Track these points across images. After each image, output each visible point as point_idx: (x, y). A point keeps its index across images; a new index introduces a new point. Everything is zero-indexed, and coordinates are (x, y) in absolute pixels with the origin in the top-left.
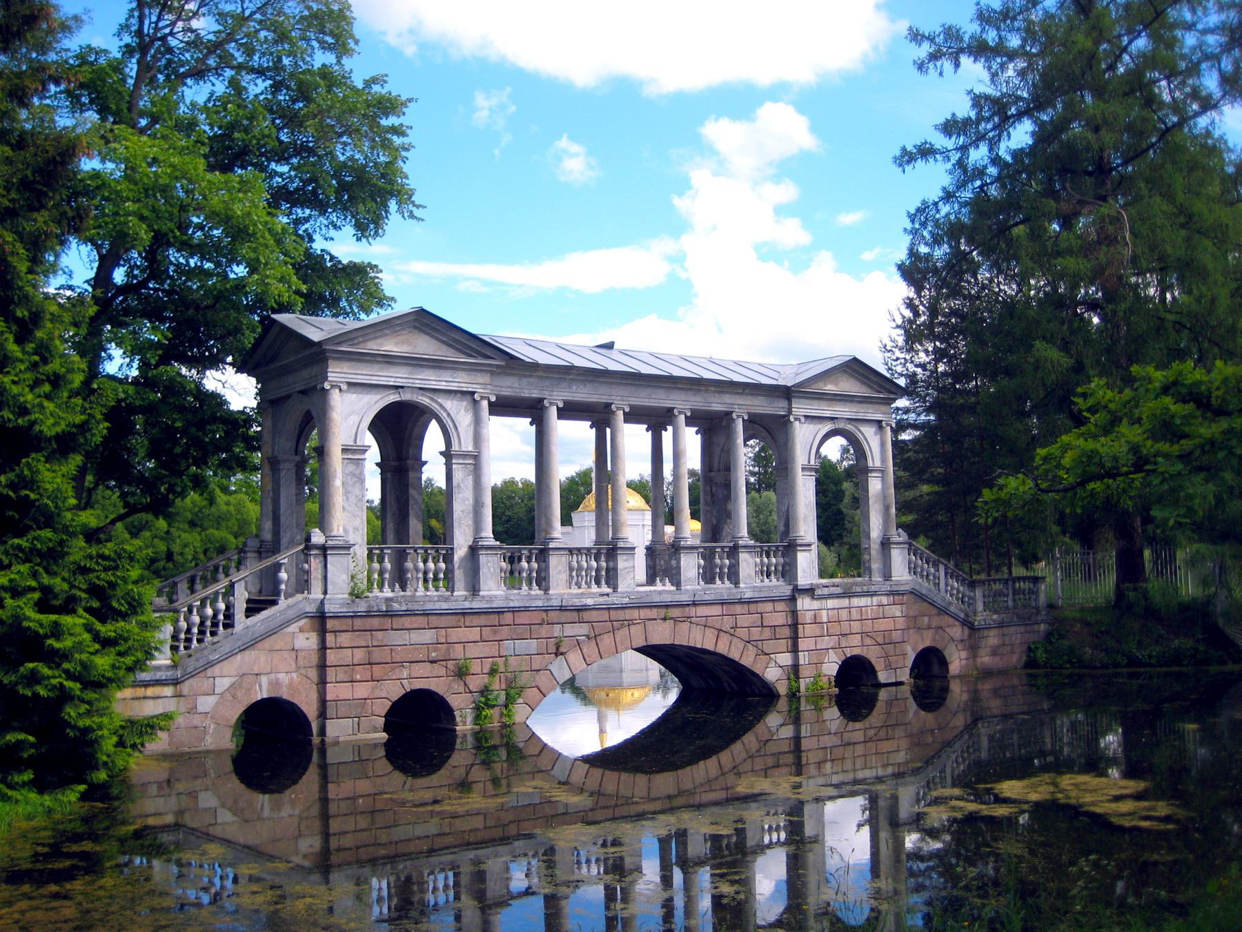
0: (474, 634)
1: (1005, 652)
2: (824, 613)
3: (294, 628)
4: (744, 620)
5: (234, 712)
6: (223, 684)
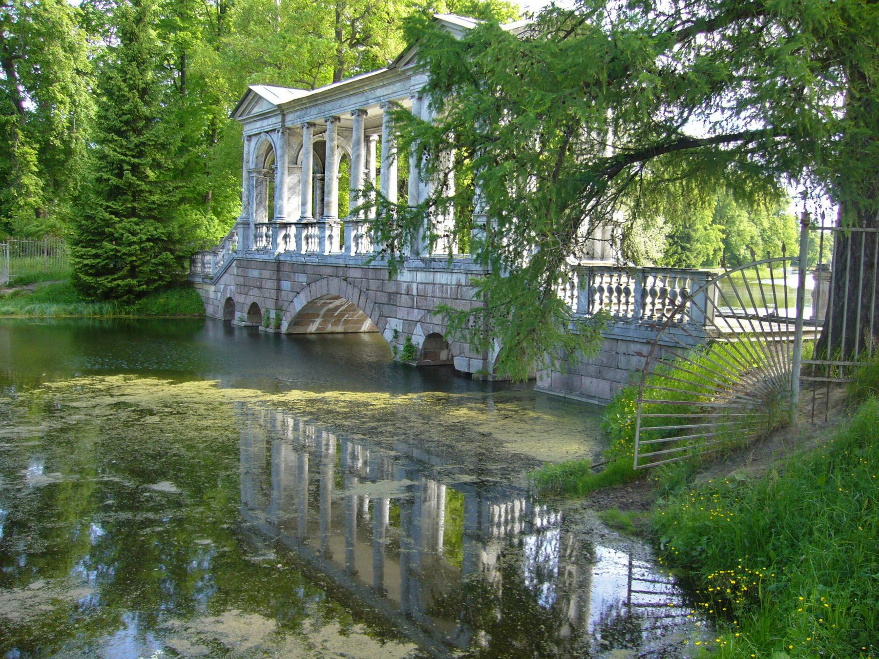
0: (266, 274)
1: (618, 377)
2: (414, 286)
3: (234, 264)
4: (374, 285)
5: (223, 301)
6: (222, 287)
